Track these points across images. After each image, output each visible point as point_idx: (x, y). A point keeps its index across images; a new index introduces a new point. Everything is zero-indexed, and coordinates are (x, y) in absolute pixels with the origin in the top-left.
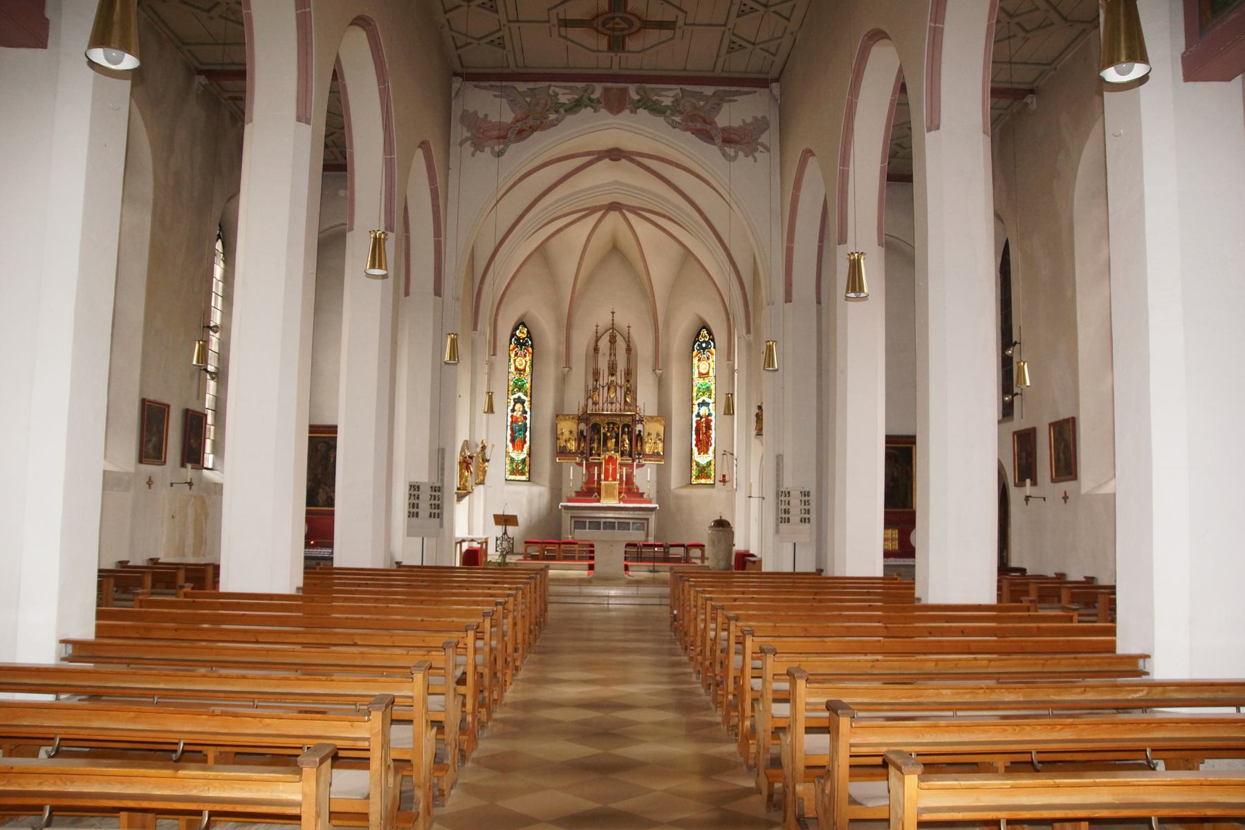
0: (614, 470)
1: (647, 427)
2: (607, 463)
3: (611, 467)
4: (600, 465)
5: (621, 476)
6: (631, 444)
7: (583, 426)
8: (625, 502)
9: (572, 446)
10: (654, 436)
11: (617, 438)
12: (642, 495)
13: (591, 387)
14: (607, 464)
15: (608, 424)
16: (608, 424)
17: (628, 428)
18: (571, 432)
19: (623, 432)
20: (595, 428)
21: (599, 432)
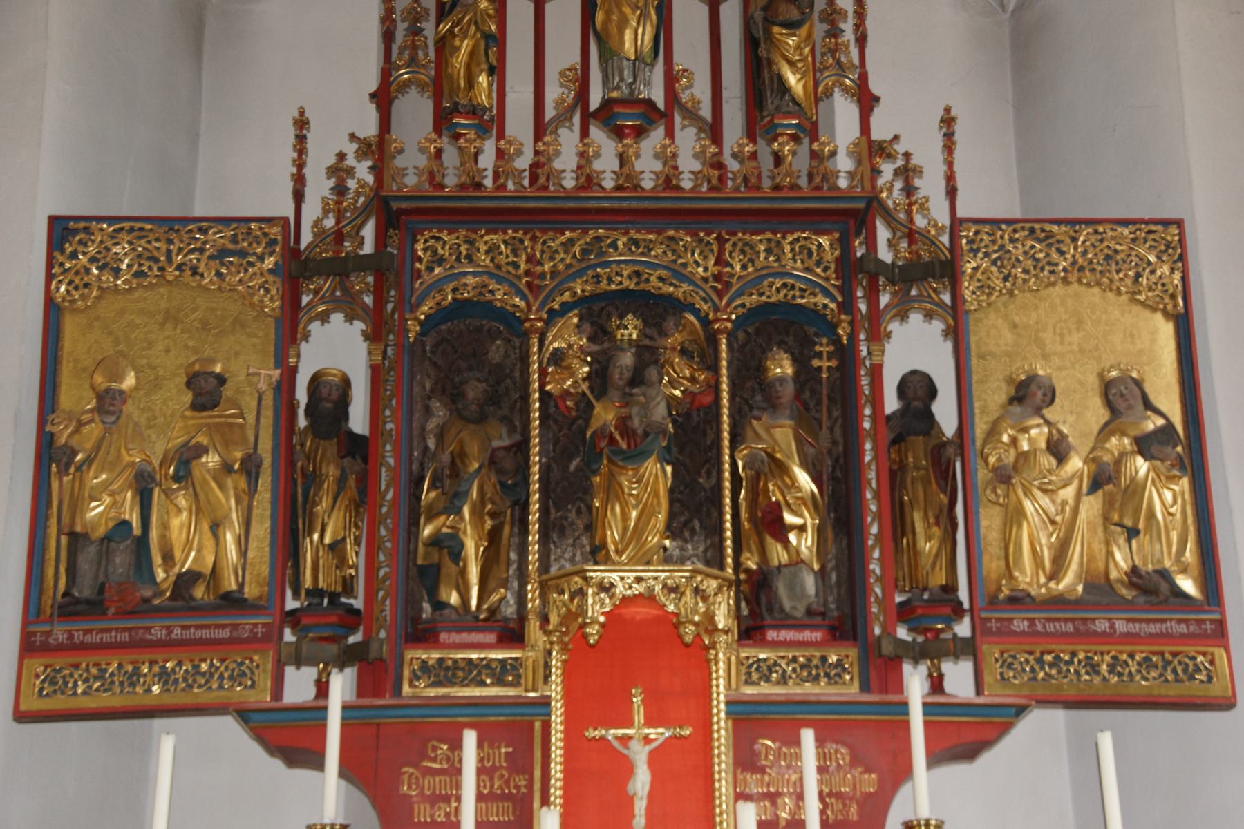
1: (992, 332)
2: (596, 699)
3: (640, 739)
4: (515, 733)
6: (839, 512)
7: (337, 347)
9: (214, 538)
10: (1080, 414)
11: (692, 443)
14: (596, 699)
16: (598, 312)
18: (206, 392)
21: (505, 396)
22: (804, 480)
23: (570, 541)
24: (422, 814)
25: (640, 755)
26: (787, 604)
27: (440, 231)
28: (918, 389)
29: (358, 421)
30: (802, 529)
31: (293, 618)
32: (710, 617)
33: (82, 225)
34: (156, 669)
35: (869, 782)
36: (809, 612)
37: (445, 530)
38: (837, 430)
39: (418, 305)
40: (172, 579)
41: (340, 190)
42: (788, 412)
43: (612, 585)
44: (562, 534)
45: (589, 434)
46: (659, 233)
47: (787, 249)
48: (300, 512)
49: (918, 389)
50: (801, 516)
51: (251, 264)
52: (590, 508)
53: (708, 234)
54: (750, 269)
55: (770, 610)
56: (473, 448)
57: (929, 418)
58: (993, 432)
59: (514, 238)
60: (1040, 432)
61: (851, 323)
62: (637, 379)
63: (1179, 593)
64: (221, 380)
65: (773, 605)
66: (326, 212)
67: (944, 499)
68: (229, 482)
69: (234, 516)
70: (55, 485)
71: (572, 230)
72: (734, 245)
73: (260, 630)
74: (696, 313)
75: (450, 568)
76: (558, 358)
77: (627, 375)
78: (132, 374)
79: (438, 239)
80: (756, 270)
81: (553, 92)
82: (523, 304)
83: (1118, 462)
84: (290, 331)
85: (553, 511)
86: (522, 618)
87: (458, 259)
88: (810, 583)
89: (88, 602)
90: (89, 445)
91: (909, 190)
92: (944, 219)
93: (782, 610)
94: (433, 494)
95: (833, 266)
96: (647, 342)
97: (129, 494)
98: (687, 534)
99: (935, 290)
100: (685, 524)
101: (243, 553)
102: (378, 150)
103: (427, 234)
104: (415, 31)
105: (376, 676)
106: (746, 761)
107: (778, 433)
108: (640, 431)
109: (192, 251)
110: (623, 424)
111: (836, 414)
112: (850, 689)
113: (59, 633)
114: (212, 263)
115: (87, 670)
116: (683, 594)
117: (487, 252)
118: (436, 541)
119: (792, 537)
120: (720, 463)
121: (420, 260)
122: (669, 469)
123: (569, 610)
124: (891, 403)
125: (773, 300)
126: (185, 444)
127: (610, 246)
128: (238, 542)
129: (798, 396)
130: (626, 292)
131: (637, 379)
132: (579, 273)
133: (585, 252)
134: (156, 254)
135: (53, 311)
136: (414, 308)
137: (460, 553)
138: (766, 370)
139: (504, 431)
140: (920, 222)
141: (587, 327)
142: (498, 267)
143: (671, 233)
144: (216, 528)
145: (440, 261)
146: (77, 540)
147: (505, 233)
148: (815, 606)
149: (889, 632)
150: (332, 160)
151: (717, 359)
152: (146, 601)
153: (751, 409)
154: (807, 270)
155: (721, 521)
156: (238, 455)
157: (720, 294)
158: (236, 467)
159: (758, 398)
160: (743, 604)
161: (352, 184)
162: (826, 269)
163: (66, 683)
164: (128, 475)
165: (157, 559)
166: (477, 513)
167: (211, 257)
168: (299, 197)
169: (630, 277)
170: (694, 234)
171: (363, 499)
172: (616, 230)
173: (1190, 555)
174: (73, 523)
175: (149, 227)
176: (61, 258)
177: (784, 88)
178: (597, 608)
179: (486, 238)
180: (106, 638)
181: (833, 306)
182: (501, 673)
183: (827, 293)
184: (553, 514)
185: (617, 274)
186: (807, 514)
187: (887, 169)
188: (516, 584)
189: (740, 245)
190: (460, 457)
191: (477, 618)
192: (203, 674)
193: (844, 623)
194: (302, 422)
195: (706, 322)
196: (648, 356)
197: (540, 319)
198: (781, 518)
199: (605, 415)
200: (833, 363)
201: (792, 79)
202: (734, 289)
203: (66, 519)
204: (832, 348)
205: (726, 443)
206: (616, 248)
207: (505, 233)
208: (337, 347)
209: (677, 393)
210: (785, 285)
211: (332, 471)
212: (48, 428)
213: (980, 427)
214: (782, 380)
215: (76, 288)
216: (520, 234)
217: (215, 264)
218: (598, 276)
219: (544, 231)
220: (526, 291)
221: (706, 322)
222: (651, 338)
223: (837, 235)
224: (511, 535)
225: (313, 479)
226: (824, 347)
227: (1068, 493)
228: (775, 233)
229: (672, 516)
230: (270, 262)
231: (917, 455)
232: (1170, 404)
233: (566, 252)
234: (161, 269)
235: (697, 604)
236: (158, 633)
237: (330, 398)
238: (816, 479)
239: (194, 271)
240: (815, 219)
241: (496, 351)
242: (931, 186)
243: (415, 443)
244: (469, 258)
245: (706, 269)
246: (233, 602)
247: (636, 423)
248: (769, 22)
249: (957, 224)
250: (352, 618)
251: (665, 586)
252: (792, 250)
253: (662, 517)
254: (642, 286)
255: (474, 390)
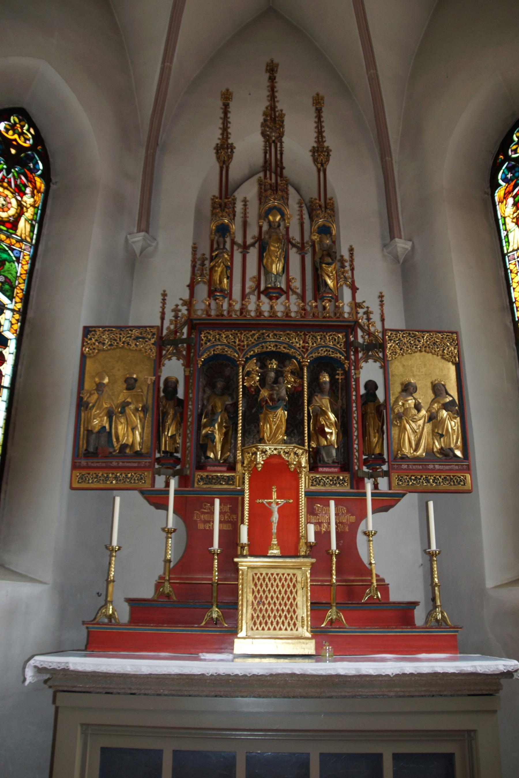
0: (290, 514)
1: (397, 367)
2: (260, 490)
3: (275, 503)
5: (323, 537)
7: (174, 368)
8: (345, 648)
9: (131, 432)
10: (424, 395)
11: (294, 404)
12: (404, 613)
13: (205, 249)
14: (260, 490)
15: (263, 358)
16: (263, 358)
17: (333, 374)
18: (131, 384)
19: (315, 387)
20: (217, 373)
22: (332, 416)
23: (252, 437)
24: (201, 526)
25: (275, 508)
26: (326, 459)
27: (210, 330)
28: (371, 386)
29: (180, 394)
30: (331, 434)
31: (158, 460)
32: (299, 463)
33: (93, 329)
34: (114, 476)
35: (352, 519)
36: (334, 462)
37: (209, 432)
38: (344, 399)
39: (202, 355)
40: (119, 446)
41: (176, 317)
42: (327, 394)
43: (266, 451)
44: (250, 434)
45: (259, 400)
46: (284, 332)
47: (328, 338)
48: (161, 425)
49: (371, 386)
50: (331, 429)
51: (146, 341)
52: (259, 425)
53: (301, 332)
54: (315, 345)
55: (320, 461)
56: (219, 404)
57: (375, 396)
58: (396, 401)
59: (234, 333)
60: (411, 402)
61: (349, 364)
62: (276, 381)
63: (456, 456)
64: (136, 380)
65: (322, 460)
66: (171, 324)
67: (380, 424)
68: (138, 415)
69: (139, 426)
70: (83, 414)
71: (254, 331)
72: (309, 336)
73: (147, 464)
74: (296, 359)
75: (210, 445)
76: (248, 374)
77: (272, 380)
78: (107, 378)
79: (209, 333)
80: (317, 345)
81: (249, 284)
82: (237, 355)
83: (437, 412)
84: (158, 364)
85: (246, 426)
86: (235, 462)
87: (215, 340)
88: (334, 452)
89: (92, 453)
90: (93, 401)
91: (368, 319)
92: (380, 329)
93: (324, 461)
94: (205, 420)
95: (343, 344)
96: (279, 369)
97: (105, 418)
98: (292, 435)
99: (377, 353)
100: (292, 431)
101: (142, 438)
102: (189, 304)
103: (205, 332)
104: (203, 265)
105: (185, 481)
106: (311, 511)
107: (324, 401)
108: (276, 399)
109: (128, 337)
110: (271, 397)
111: (344, 394)
112: (346, 488)
113: (83, 462)
114: (133, 341)
115: (92, 475)
116: (290, 454)
117: (225, 338)
118: (207, 435)
119: (328, 436)
120: (304, 411)
121: (202, 340)
122: (286, 413)
123: (251, 459)
124: (362, 391)
125: (323, 355)
126: (124, 401)
127: (267, 336)
128: (140, 434)
129: (331, 388)
130: (273, 352)
131: (276, 381)
132: (257, 345)
133: (258, 338)
134: (116, 338)
135: (83, 357)
136: (200, 356)
137: (214, 440)
138: (320, 379)
139: (230, 398)
140: (372, 329)
141: (259, 364)
142: (229, 343)
143: (288, 332)
144: (133, 429)
145: (209, 341)
146: (89, 432)
147: (231, 331)
148: (335, 460)
149: (360, 468)
150: (173, 307)
151: (303, 375)
152: (111, 453)
153: (315, 392)
154: (334, 345)
155: (304, 431)
156: (141, 405)
157: (304, 353)
158: (140, 409)
159: (317, 388)
160: (311, 459)
161: (180, 314)
162: (340, 345)
163: (86, 479)
164: (105, 411)
165: (114, 440)
166: (220, 426)
167: (134, 339)
168: (162, 319)
169: (274, 347)
170: (296, 333)
171: (181, 420)
172: (269, 330)
173: (459, 443)
174: (88, 427)
175: (114, 329)
176: (86, 340)
177: (326, 284)
178: (260, 459)
179: (225, 333)
180: (98, 465)
181: (343, 357)
182: (229, 480)
183: (341, 353)
184: (247, 427)
185: (270, 346)
186: (333, 429)
187: (361, 311)
188: (233, 451)
189: (311, 336)
190: (214, 407)
191: (219, 462)
192: (129, 478)
193: (345, 465)
194: (162, 394)
195: (299, 363)
196: (279, 373)
197: (243, 361)
198: (324, 430)
199: (264, 393)
200: (343, 377)
201: (329, 282)
202: (309, 351)
203: (86, 426)
204: (342, 372)
205: (306, 404)
206: (269, 337)
207: (231, 331)
208: (174, 368)
209: (289, 386)
210: (327, 350)
211: (171, 412)
212: (81, 395)
213: (392, 399)
214: (325, 382)
215: (91, 350)
216: (236, 332)
217: (135, 342)
218: (262, 346)
219: (245, 331)
220: (238, 351)
221: (299, 363)
222: (281, 368)
223: (344, 334)
224: (232, 434)
225: (165, 414)
226: (340, 372)
227: (421, 422)
228: (323, 332)
229: (287, 428)
230: (153, 341)
231: (371, 408)
232: (454, 392)
233: (252, 338)
234: (117, 343)
235: (295, 458)
236: (114, 464)
237: (171, 387)
238: (336, 416)
239: (128, 344)
240: (338, 328)
241: (228, 372)
242: (375, 317)
243: (200, 403)
244: (219, 340)
245: (300, 344)
246: (138, 454)
247: (275, 396)
248: (321, 263)
249: (384, 331)
250: (178, 461)
251: (284, 452)
252: (329, 338)
253: (284, 428)
254: (278, 350)
255: (220, 385)
